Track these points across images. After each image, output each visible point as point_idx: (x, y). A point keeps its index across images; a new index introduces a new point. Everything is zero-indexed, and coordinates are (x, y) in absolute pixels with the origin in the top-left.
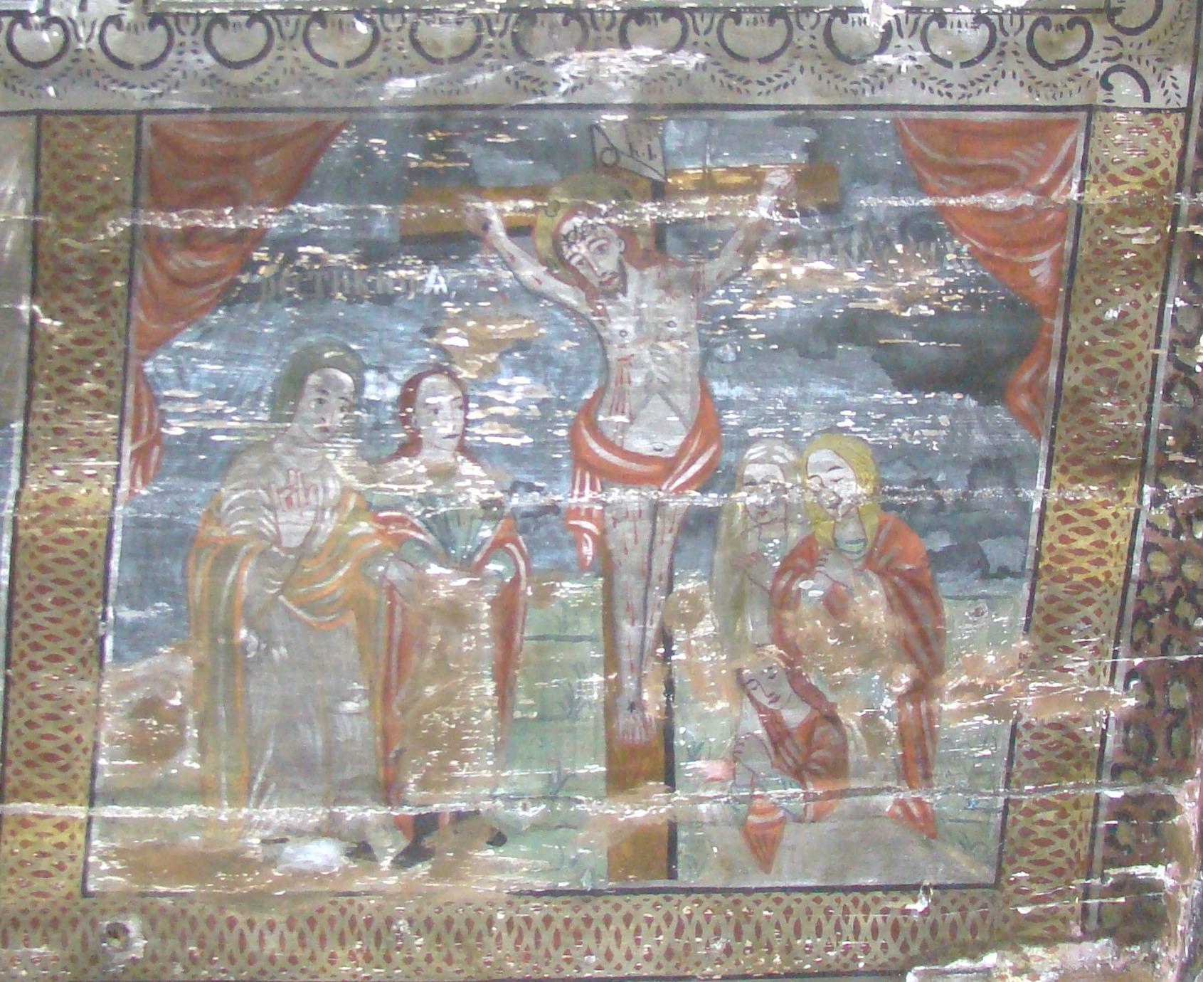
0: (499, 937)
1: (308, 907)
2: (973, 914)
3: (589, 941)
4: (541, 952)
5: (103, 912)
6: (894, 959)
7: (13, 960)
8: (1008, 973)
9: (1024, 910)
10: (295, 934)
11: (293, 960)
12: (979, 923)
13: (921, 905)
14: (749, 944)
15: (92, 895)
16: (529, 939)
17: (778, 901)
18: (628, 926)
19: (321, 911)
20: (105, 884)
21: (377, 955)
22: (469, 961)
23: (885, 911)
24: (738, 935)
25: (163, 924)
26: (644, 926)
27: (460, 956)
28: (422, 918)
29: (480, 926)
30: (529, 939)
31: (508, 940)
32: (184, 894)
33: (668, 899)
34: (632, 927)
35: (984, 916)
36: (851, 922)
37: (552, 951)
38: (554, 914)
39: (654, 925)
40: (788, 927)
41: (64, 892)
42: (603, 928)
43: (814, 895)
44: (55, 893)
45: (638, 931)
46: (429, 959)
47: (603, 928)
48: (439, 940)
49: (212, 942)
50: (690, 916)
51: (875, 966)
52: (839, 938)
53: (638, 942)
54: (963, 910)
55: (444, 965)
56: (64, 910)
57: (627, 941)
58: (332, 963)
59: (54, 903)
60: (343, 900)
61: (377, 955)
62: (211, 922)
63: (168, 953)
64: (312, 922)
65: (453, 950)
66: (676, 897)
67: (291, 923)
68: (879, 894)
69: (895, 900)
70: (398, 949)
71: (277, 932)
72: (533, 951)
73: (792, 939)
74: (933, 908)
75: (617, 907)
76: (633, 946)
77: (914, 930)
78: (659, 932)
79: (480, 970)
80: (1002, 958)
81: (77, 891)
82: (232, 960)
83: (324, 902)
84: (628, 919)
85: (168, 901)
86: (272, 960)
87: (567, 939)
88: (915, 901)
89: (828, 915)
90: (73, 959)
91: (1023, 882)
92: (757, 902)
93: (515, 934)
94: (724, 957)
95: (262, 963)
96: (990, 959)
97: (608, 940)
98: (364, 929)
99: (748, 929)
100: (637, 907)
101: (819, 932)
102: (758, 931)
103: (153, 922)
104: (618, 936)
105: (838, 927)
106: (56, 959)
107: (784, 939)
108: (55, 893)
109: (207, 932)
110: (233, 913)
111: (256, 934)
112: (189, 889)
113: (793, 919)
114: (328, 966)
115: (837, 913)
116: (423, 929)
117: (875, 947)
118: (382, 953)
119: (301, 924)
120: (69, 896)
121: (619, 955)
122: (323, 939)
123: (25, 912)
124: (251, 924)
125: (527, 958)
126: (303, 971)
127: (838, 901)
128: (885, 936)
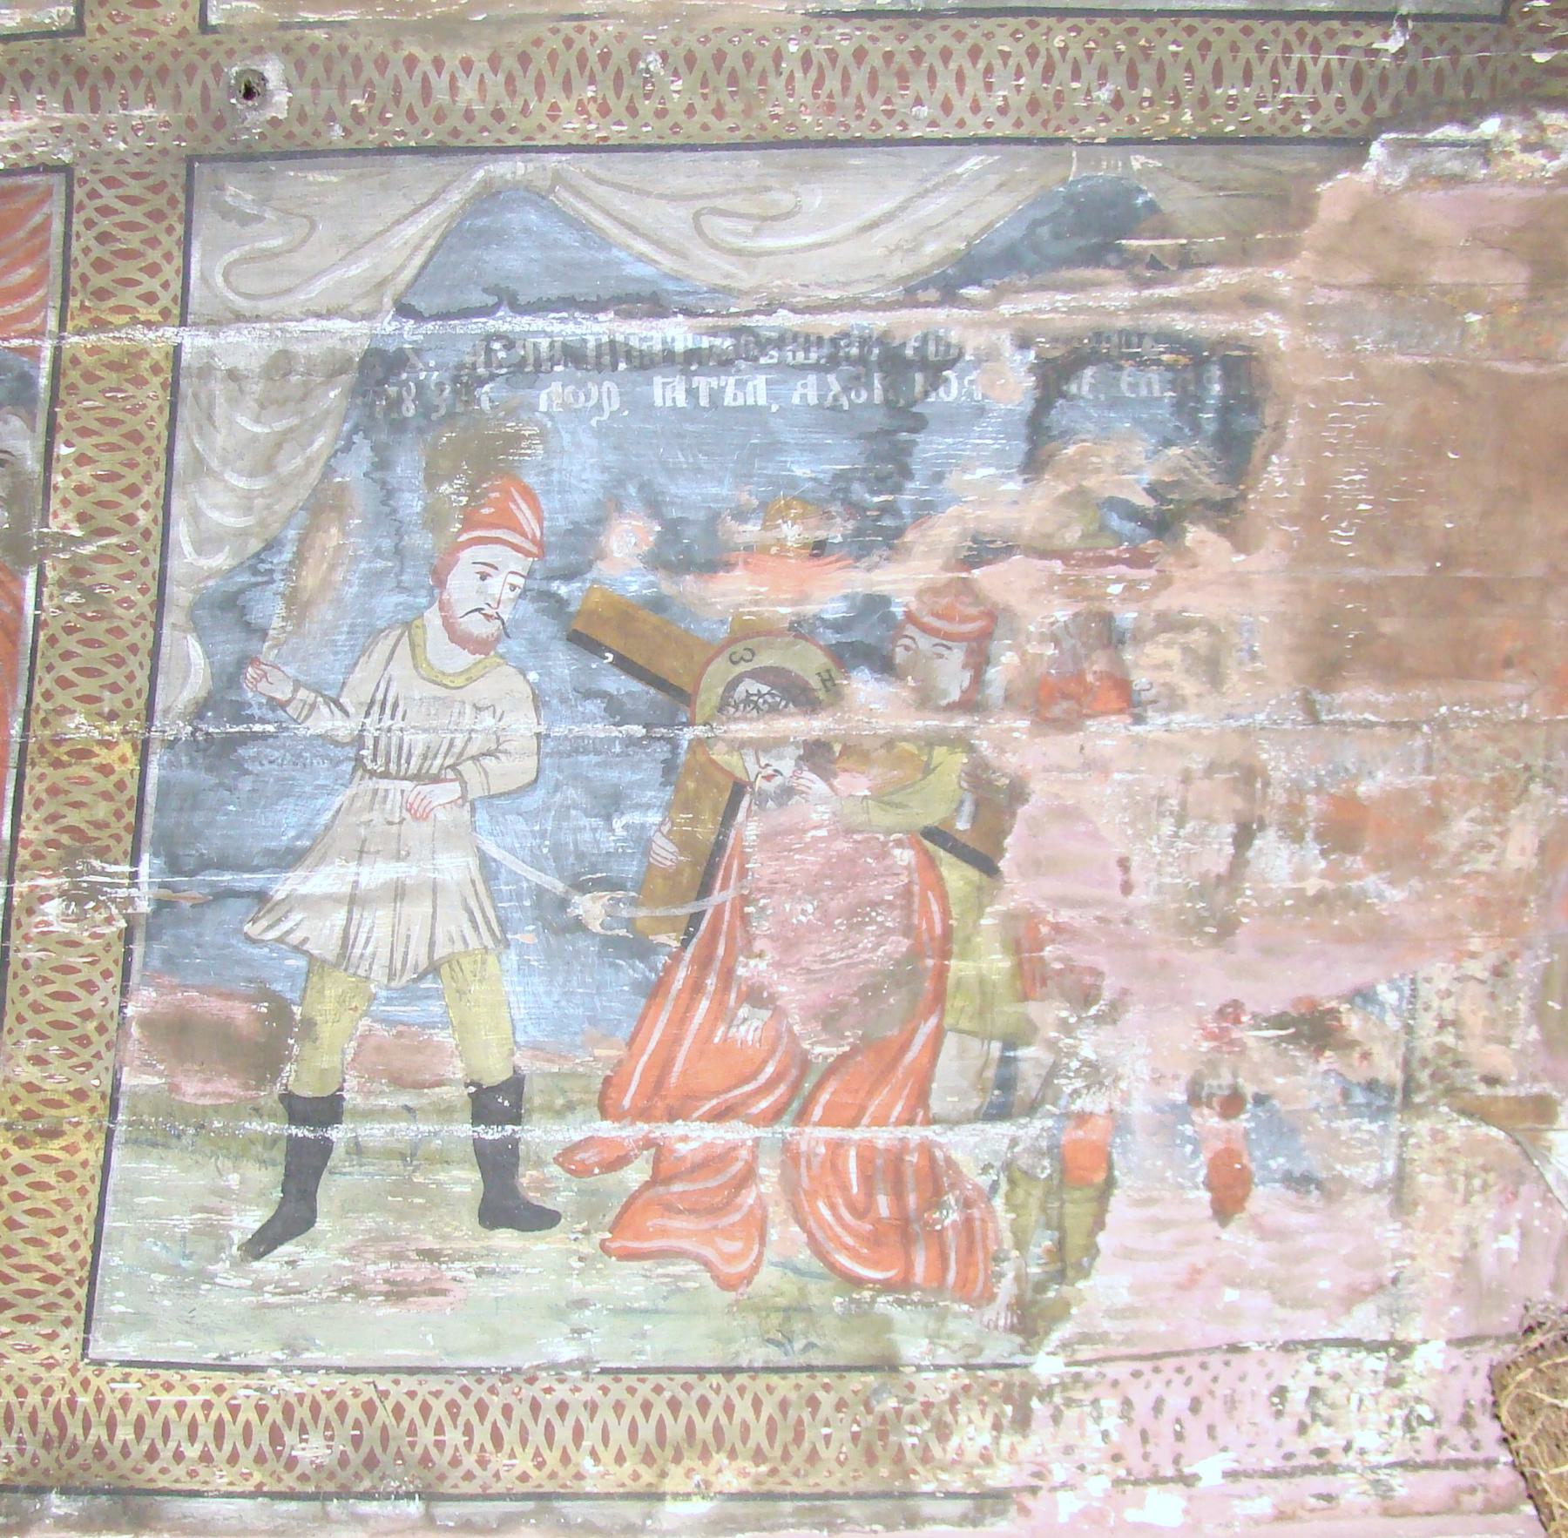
0: (791, 77)
1: (519, 38)
2: (1468, 59)
3: (919, 84)
4: (851, 100)
5: (230, 53)
6: (1353, 123)
7: (106, 129)
8: (1515, 148)
9: (1540, 58)
10: (501, 78)
11: (498, 115)
12: (1475, 71)
13: (1394, 44)
14: (1147, 93)
15: (214, 30)
16: (833, 83)
17: (1190, 30)
18: (974, 63)
19: (538, 42)
20: (232, 14)
21: (618, 106)
22: (747, 112)
23: (1343, 50)
24: (1133, 79)
25: (315, 67)
26: (997, 63)
27: (734, 107)
28: (681, 51)
29: (763, 61)
30: (833, 83)
31: (803, 84)
32: (342, 24)
33: (1033, 25)
34: (981, 65)
35: (1483, 62)
36: (1294, 65)
37: (866, 99)
38: (868, 45)
39: (1012, 62)
40: (1204, 69)
41: (175, 28)
42: (939, 67)
43: (1241, 23)
44: (162, 29)
45: (989, 71)
46: (690, 111)
47: (939, 67)
48: (704, 84)
49: (383, 90)
50: (1064, 51)
51: (1326, 131)
52: (1277, 88)
53: (989, 87)
54: (1454, 52)
55: (711, 120)
56: (176, 54)
57: (974, 86)
58: (553, 118)
59: (162, 44)
60: (568, 27)
61: (618, 106)
62: (382, 64)
63: (322, 111)
64: (524, 60)
65: (725, 98)
66: (1045, 22)
67: (494, 62)
68: (1336, 24)
69: (1357, 34)
70: (647, 96)
71: (475, 77)
72: (838, 100)
73: (1209, 87)
74: (1411, 47)
75: (960, 36)
76: (982, 94)
77: (1383, 80)
78: (1019, 74)
79: (763, 128)
80: (1507, 126)
81: (193, 27)
82: (411, 116)
83: (542, 30)
84: (975, 53)
85: (320, 35)
86: (469, 115)
87: (888, 82)
88: (1386, 37)
89: (1262, 54)
90: (190, 123)
91: (1542, 15)
92: (1161, 32)
93: (813, 74)
94: (1111, 112)
95: (455, 120)
96: (1490, 127)
97: (946, 83)
98: (598, 68)
99: (1147, 71)
100: (989, 36)
101: (1248, 78)
102: (1161, 76)
103: (300, 66)
104: (960, 77)
105: (1274, 73)
106: (166, 124)
107: (1197, 89)
108: (162, 29)
109: (376, 76)
110: (417, 51)
111: (445, 77)
112: (350, 15)
113: (1211, 58)
114: (546, 122)
115: (1274, 52)
116: (683, 69)
117: (1328, 101)
118: (624, 101)
119: (510, 62)
120: (183, 33)
121: (961, 106)
122: (540, 84)
123: (120, 59)
124: (438, 64)
125: (831, 108)
126: (512, 130)
127: (1276, 32)
128: (1341, 87)
